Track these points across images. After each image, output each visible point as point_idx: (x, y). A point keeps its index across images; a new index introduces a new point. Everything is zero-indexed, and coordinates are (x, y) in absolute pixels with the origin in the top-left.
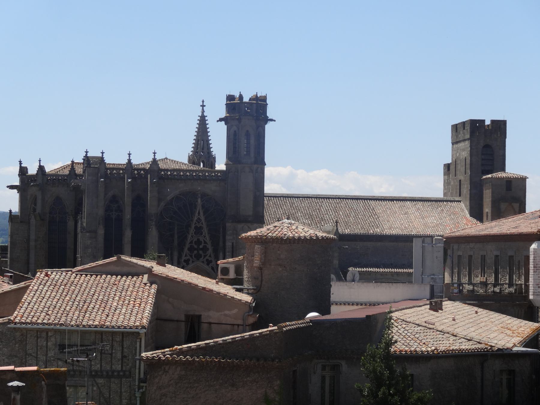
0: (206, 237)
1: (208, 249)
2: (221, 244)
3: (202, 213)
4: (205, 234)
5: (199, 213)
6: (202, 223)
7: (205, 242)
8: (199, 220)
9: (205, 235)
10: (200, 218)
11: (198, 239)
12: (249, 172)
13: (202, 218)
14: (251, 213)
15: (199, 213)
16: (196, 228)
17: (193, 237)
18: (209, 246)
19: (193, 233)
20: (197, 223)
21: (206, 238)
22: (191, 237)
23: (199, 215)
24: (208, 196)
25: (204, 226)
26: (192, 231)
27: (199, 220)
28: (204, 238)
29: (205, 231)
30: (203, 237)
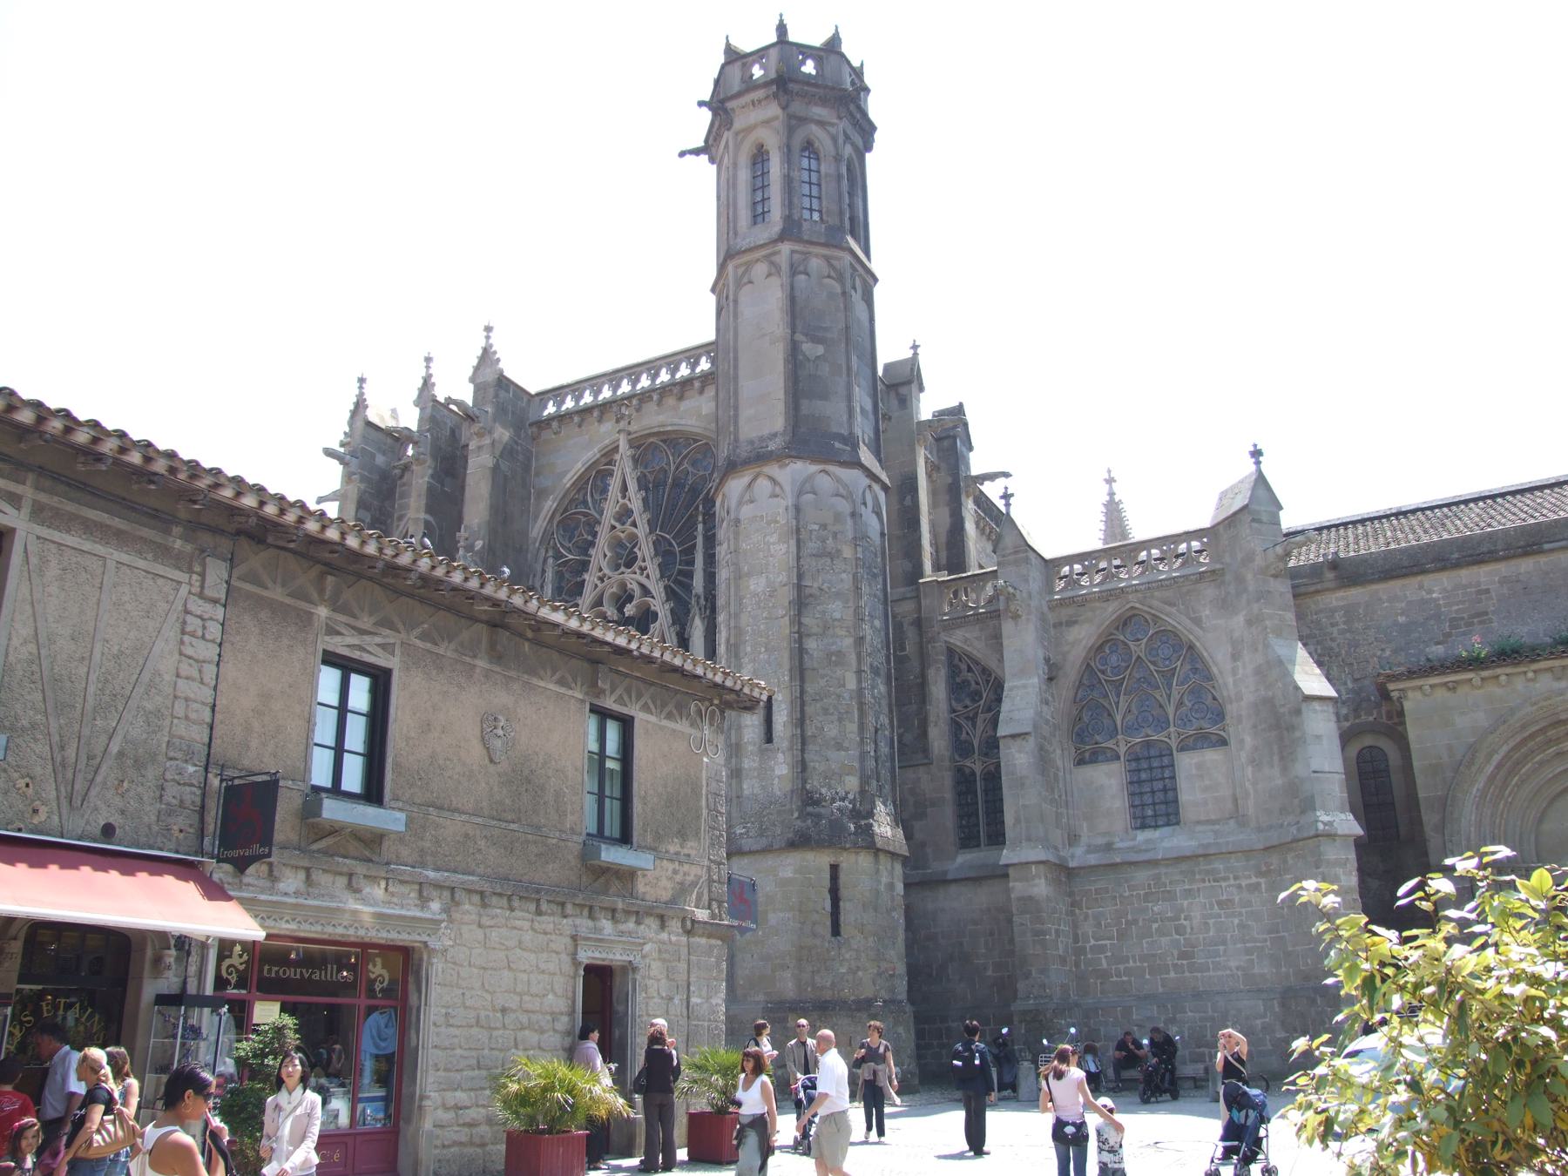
0: (648, 577)
1: (655, 616)
2: (698, 582)
3: (632, 486)
4: (644, 561)
5: (624, 489)
6: (634, 525)
7: (646, 591)
8: (624, 514)
9: (643, 564)
10: (628, 502)
11: (623, 586)
12: (769, 275)
13: (636, 504)
14: (779, 423)
15: (624, 489)
16: (617, 544)
17: (603, 581)
18: (660, 605)
19: (604, 564)
20: (617, 525)
21: (648, 577)
22: (598, 582)
23: (624, 497)
24: (696, 441)
25: (642, 531)
26: (600, 554)
27: (624, 514)
28: (642, 574)
29: (645, 550)
30: (638, 571)
